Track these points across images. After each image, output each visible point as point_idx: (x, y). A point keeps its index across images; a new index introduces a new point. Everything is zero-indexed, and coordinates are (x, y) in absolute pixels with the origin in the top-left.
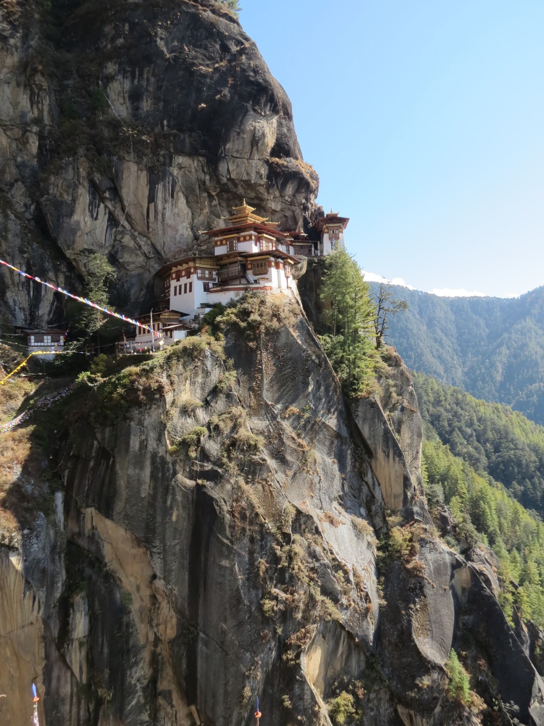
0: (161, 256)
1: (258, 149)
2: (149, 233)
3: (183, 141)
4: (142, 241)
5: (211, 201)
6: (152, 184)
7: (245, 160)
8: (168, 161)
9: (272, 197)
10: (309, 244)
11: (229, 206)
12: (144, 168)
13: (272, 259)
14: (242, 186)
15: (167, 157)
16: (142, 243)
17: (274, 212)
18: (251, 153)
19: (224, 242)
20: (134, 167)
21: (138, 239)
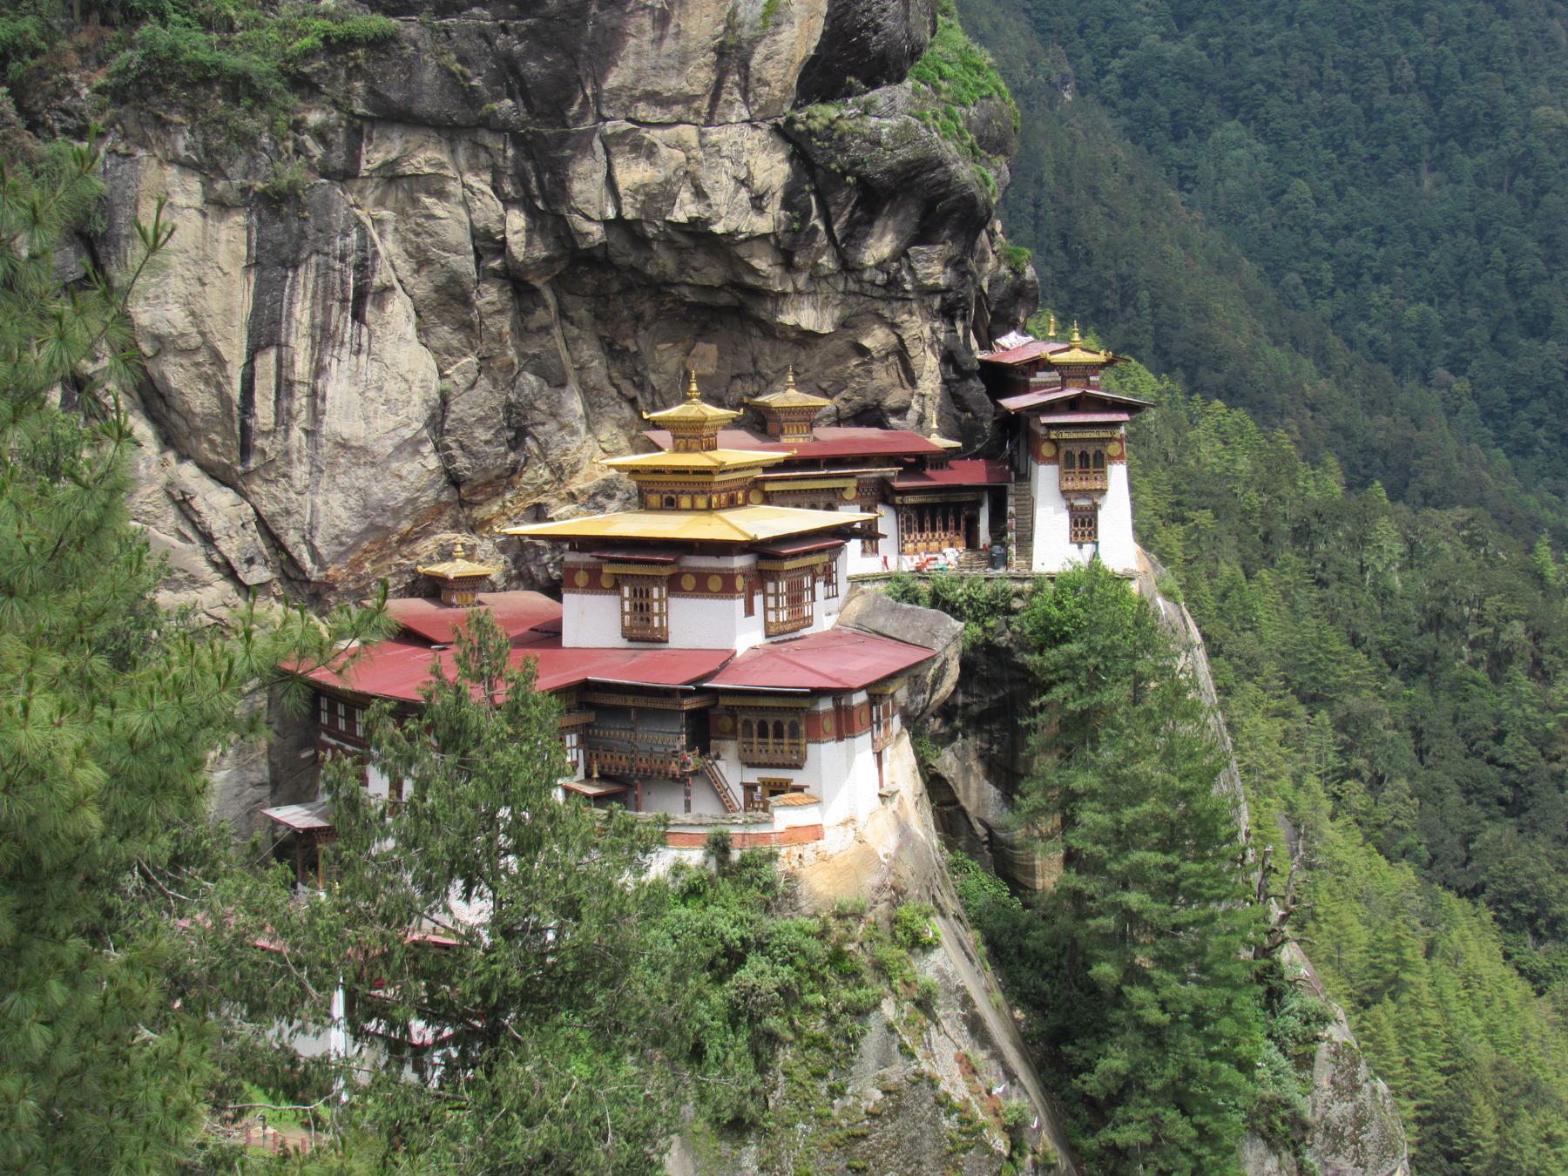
0: (302, 571)
1: (746, 78)
2: (247, 473)
3: (410, 66)
4: (217, 504)
5: (523, 312)
6: (271, 264)
7: (689, 133)
8: (338, 159)
9: (801, 281)
10: (968, 497)
11: (597, 317)
12: (232, 196)
13: (826, 705)
14: (670, 243)
15: (340, 138)
16: (216, 524)
17: (806, 338)
18: (715, 97)
19: (606, 583)
20: (187, 191)
21: (198, 504)
